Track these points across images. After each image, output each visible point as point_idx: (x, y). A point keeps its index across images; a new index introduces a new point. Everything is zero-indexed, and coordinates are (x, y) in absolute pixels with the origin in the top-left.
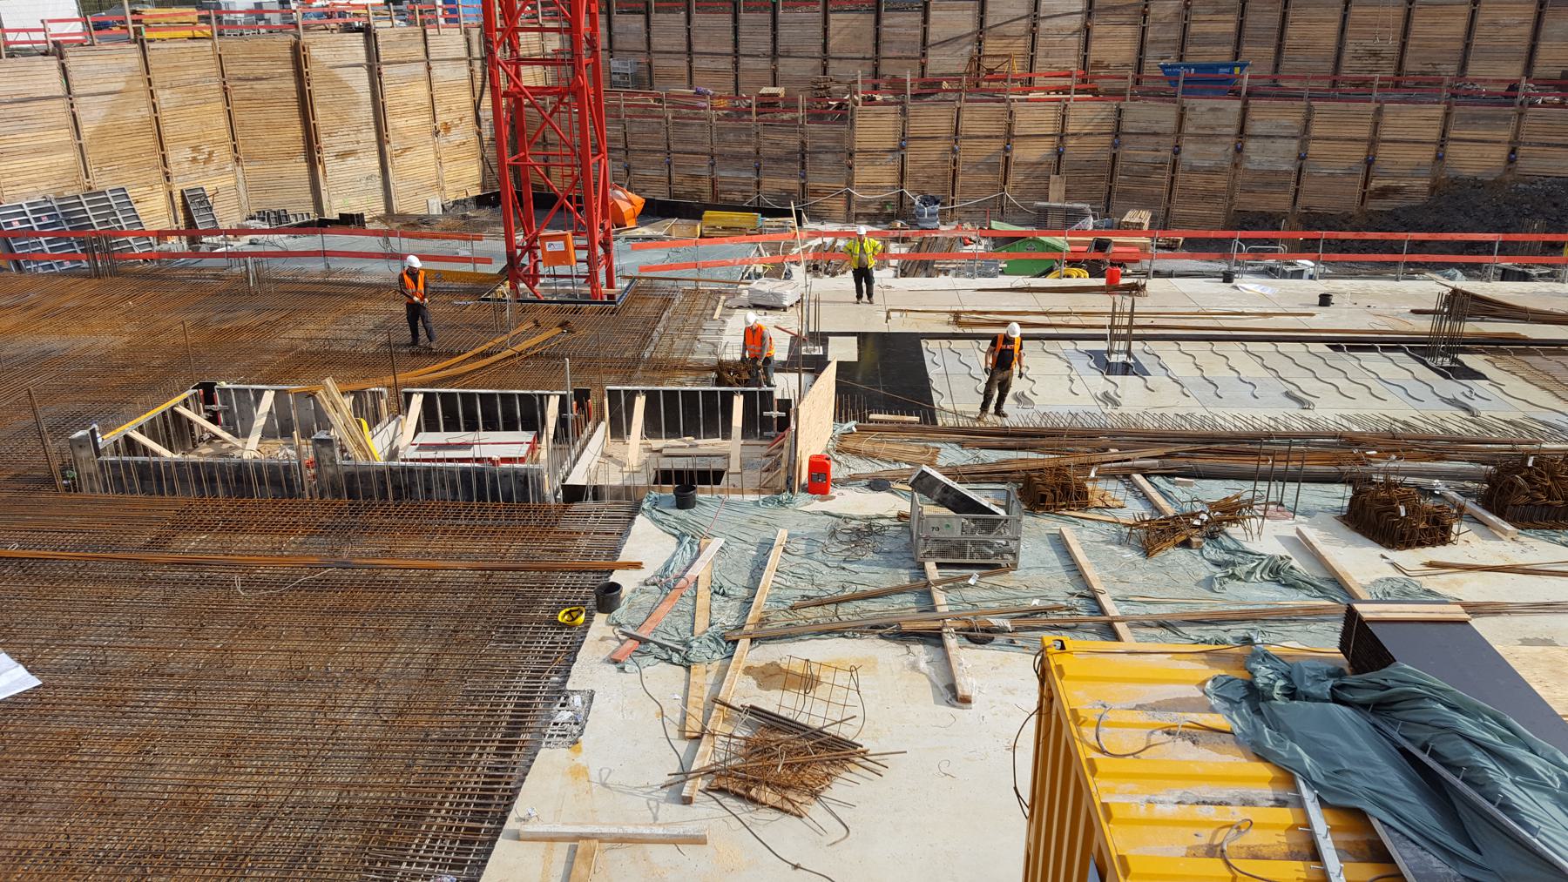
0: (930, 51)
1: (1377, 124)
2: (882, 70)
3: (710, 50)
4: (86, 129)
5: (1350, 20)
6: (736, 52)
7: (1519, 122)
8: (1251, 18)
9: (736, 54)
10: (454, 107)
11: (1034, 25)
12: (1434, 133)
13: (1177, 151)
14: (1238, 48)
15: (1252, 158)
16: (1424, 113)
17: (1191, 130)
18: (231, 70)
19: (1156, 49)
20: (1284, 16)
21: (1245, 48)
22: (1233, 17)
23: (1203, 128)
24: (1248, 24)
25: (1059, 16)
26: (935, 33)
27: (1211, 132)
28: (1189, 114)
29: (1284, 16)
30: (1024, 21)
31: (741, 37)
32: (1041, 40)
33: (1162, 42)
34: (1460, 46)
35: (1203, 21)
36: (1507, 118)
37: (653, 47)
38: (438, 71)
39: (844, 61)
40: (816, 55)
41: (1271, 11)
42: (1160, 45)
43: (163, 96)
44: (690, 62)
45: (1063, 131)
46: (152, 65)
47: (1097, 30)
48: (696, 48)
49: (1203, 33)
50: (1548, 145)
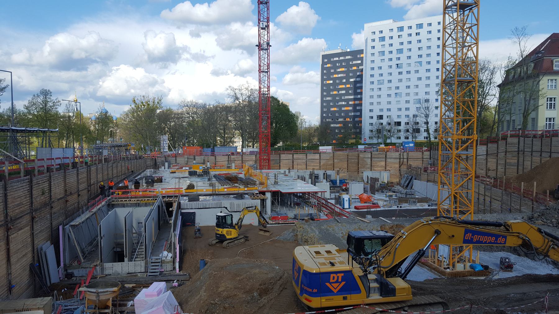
4: (322, 164)
18: (349, 157)
22: (516, 158)
33: (501, 164)
35: (510, 159)
38: (388, 160)
43: (335, 160)
46: (335, 156)
47: (489, 160)
49: (510, 162)
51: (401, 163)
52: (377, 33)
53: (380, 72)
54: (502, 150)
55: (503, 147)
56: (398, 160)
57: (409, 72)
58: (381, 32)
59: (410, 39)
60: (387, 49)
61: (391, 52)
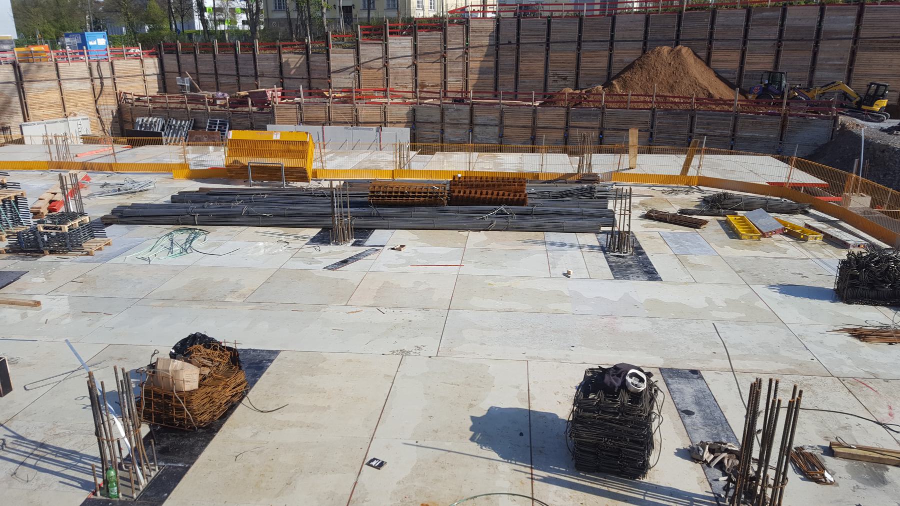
0: (332, 75)
1: (534, 118)
2: (313, 85)
3: (225, 73)
5: (549, 61)
6: (238, 74)
7: (602, 116)
8: (501, 59)
9: (238, 75)
10: (79, 104)
11: (387, 62)
12: (562, 124)
13: (442, 131)
14: (497, 76)
15: (478, 136)
16: (556, 112)
17: (448, 121)
19: (453, 76)
20: (518, 58)
21: (500, 76)
23: (453, 120)
24: (500, 62)
25: (399, 57)
26: (334, 65)
27: (457, 122)
28: (446, 113)
29: (518, 58)
30: (381, 60)
31: (240, 66)
32: (391, 71)
33: (456, 72)
34: (606, 74)
36: (597, 115)
37: (199, 72)
39: (292, 80)
40: (277, 76)
41: (510, 55)
42: (454, 74)
44: (217, 79)
45: (385, 120)
47: (419, 65)
48: (219, 72)
50: (618, 130)
51: (97, 91)
54: (456, 44)
55: (458, 39)
56: (88, 85)
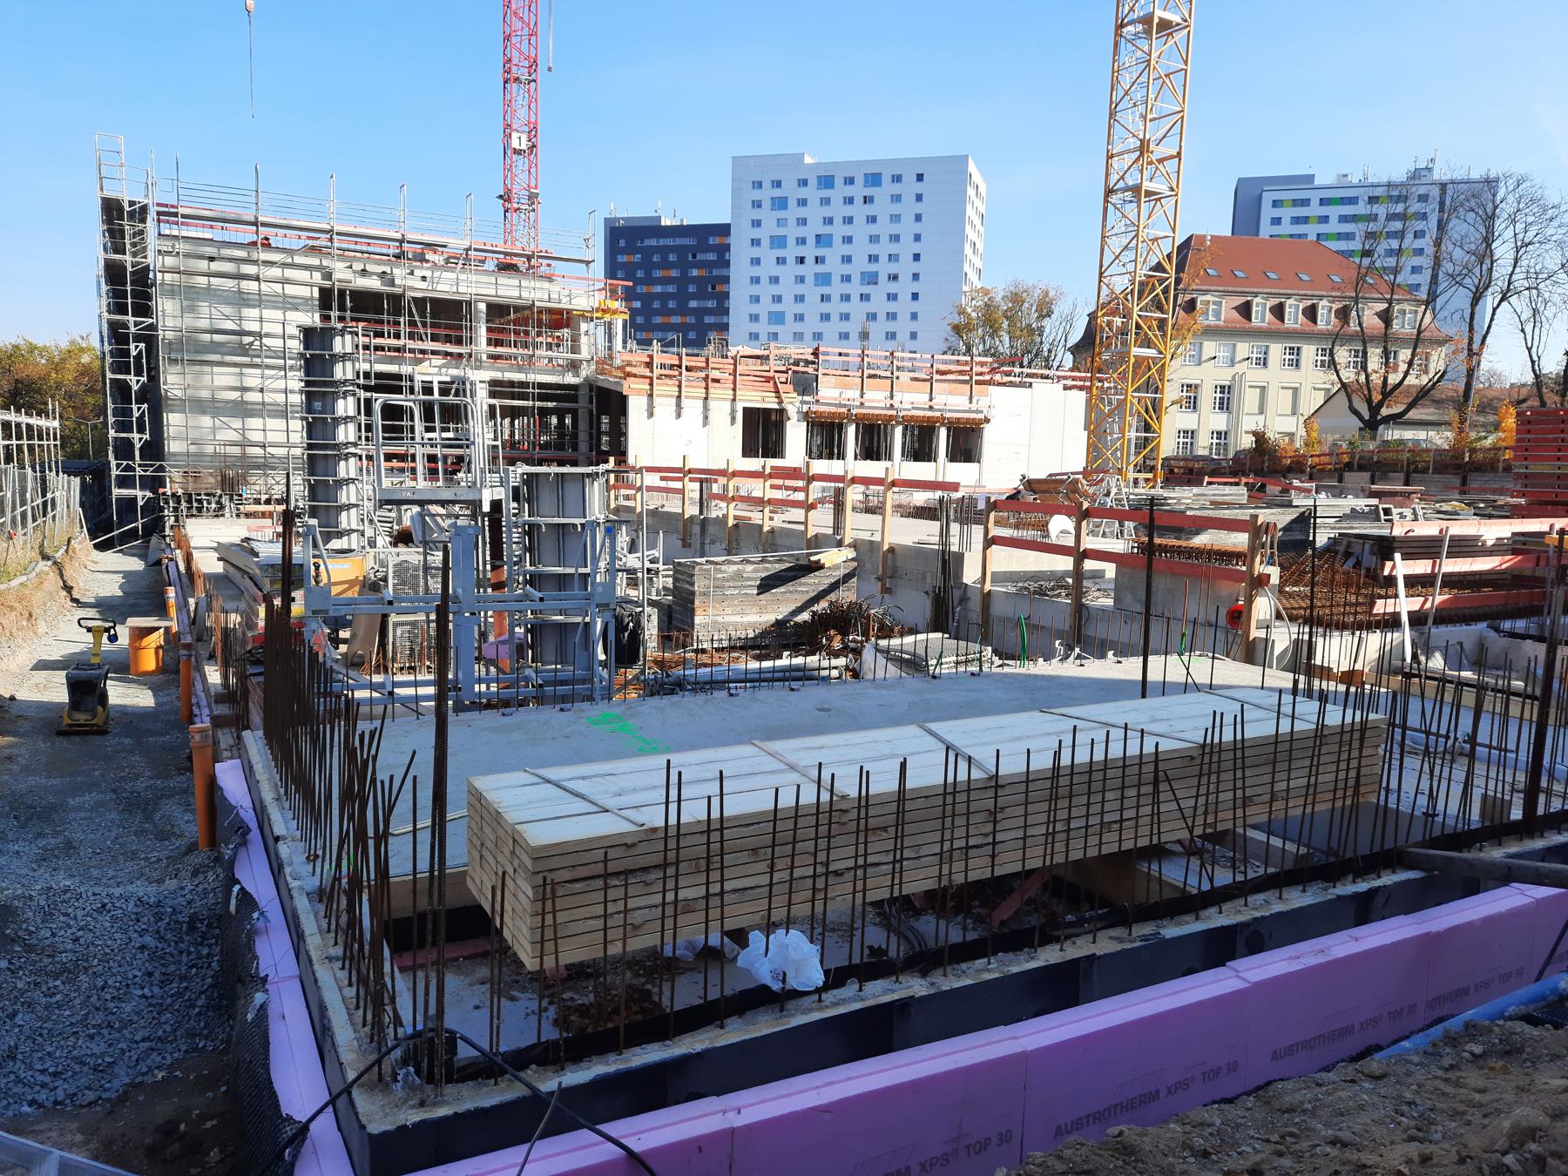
52: (767, 184)
53: (775, 290)
57: (846, 298)
58: (777, 184)
59: (848, 211)
60: (792, 232)
61: (802, 241)
